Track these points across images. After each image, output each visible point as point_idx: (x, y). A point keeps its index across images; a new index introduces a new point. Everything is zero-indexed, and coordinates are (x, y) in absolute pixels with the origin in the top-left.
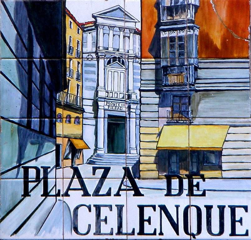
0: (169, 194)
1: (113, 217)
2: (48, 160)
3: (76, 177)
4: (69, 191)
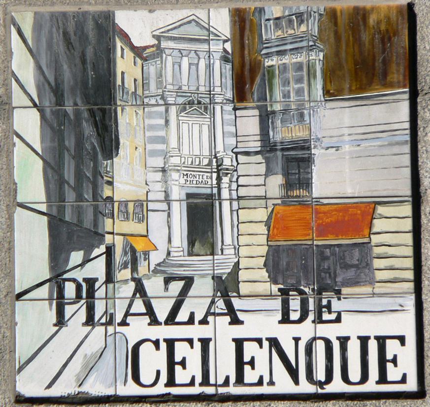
0: (285, 319)
1: (194, 356)
2: (97, 269)
3: (138, 295)
4: (128, 317)
